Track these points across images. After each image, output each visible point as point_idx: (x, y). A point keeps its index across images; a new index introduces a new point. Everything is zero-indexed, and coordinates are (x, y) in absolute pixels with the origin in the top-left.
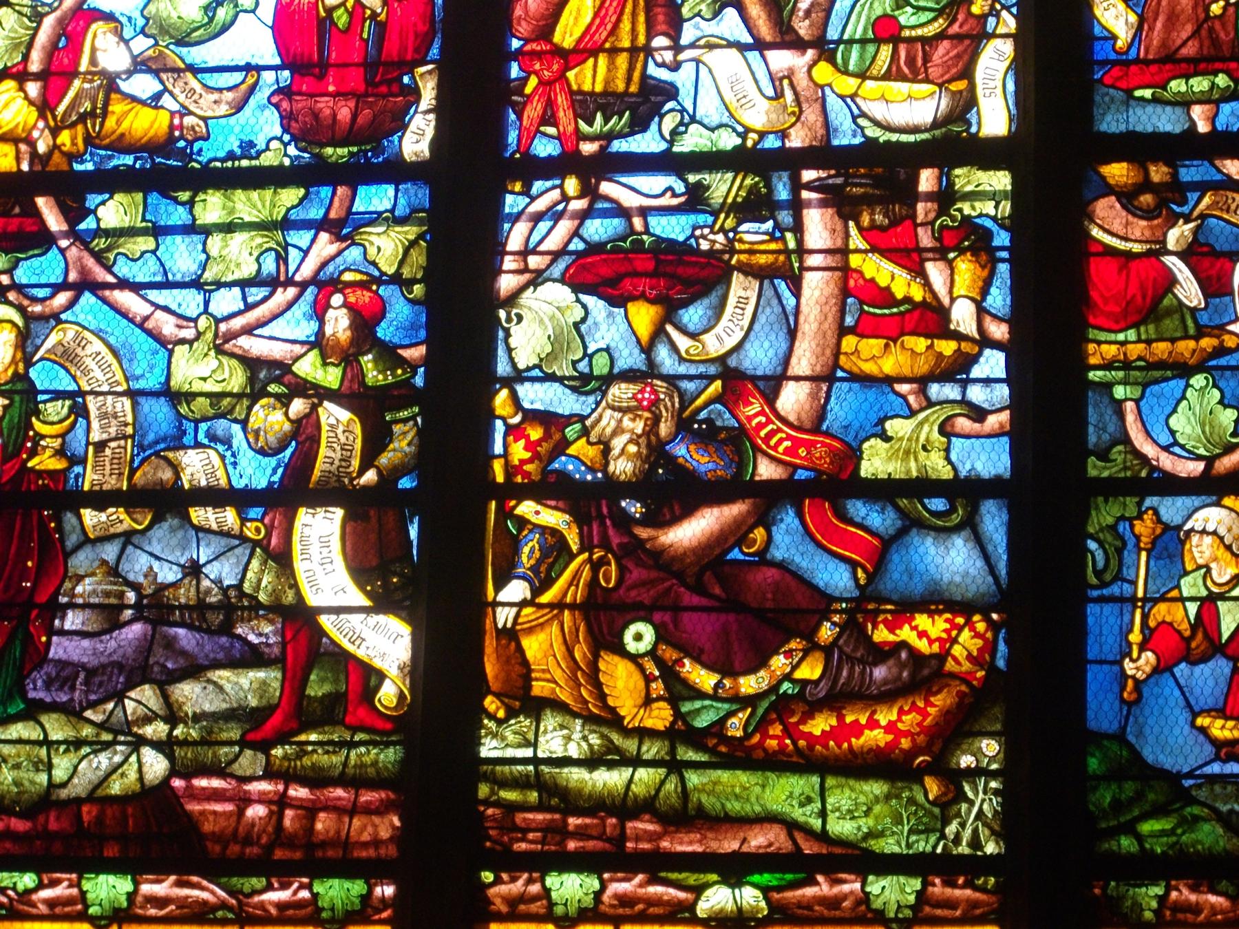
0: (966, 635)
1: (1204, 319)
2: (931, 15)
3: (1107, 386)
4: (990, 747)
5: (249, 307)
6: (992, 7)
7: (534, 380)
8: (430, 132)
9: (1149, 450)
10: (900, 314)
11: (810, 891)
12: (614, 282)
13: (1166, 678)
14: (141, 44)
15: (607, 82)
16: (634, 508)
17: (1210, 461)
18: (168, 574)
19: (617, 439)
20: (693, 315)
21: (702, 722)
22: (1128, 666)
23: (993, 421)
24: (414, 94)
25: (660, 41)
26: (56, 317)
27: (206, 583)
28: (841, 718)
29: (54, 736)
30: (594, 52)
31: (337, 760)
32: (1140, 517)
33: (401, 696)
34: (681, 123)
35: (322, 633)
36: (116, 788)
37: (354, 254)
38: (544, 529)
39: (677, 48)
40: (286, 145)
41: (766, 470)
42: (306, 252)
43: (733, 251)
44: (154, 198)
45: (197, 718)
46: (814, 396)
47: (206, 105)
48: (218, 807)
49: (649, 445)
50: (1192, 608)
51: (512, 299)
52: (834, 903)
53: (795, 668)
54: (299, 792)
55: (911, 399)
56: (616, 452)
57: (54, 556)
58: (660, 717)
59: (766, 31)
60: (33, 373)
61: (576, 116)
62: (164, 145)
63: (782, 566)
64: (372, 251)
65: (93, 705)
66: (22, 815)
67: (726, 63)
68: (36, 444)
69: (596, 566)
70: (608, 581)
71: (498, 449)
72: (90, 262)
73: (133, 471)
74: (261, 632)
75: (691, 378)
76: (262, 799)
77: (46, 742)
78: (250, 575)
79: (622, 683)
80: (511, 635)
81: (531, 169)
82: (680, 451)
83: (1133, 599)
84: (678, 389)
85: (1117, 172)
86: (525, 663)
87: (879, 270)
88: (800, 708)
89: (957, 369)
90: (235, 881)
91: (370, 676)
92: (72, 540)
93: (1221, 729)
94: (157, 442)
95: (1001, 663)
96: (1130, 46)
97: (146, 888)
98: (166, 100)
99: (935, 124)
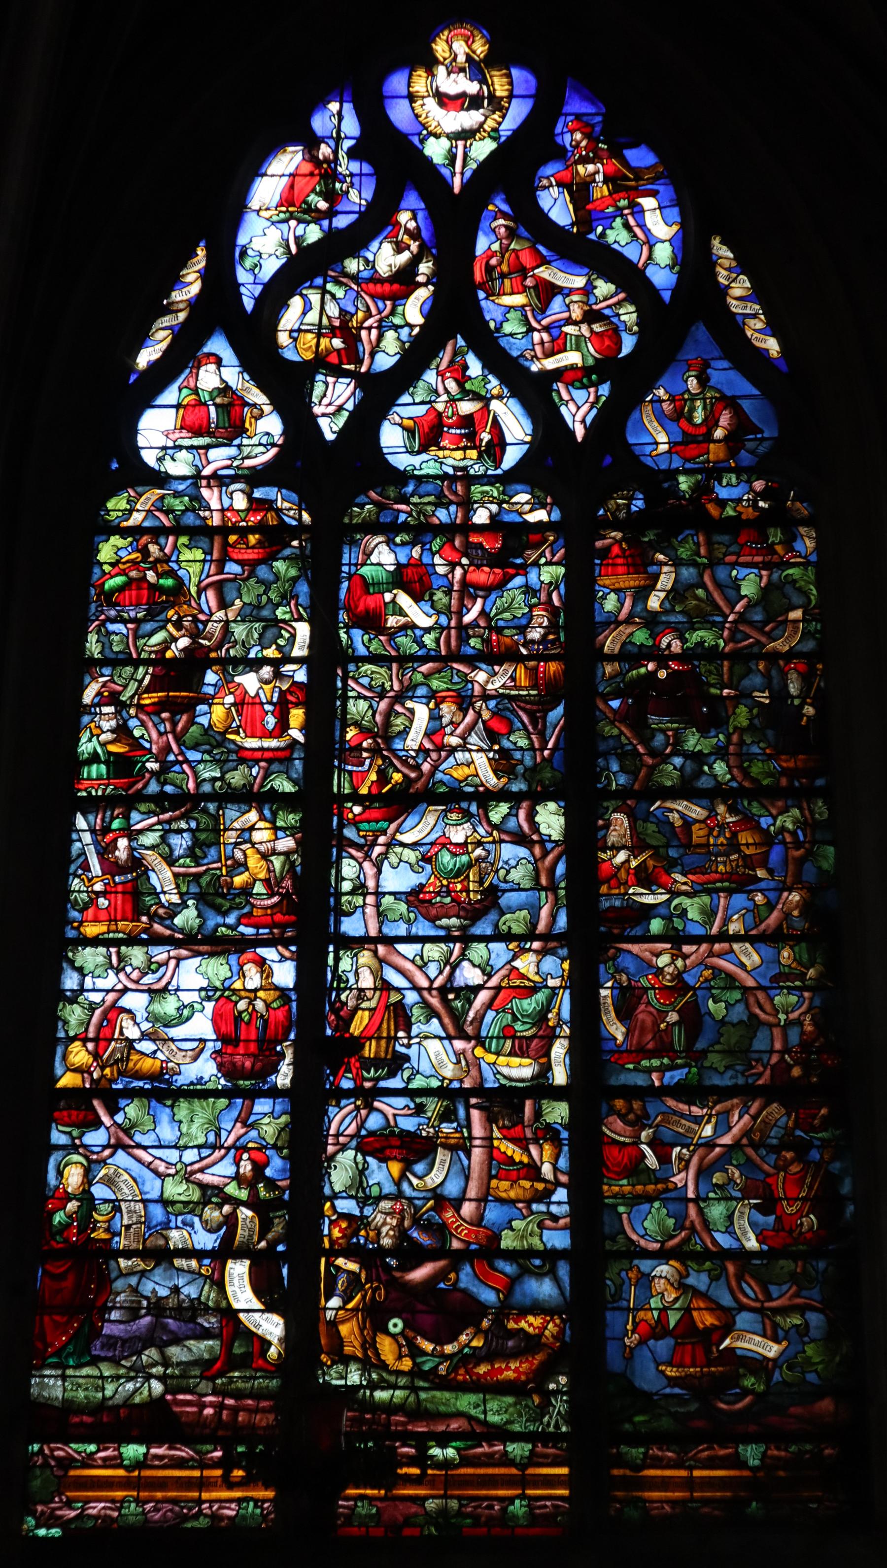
0: (550, 1326)
1: (658, 1175)
3: (615, 1206)
4: (563, 1380)
5: (202, 1159)
9: (634, 1237)
11: (480, 1450)
13: (645, 1347)
14: (146, 1026)
15: (376, 1052)
16: (393, 1263)
17: (663, 1243)
18: (163, 1292)
20: (419, 1168)
21: (426, 1367)
23: (562, 1222)
24: (282, 1056)
25: (401, 1034)
26: (104, 1162)
29: (106, 1374)
30: (370, 1039)
31: (249, 1385)
33: (279, 1354)
35: (241, 1322)
36: (137, 1399)
37: (253, 1134)
38: (349, 1272)
39: (410, 1038)
41: (456, 1245)
44: (154, 1103)
45: (179, 1364)
46: (478, 1208)
47: (179, 1058)
48: (188, 1409)
50: (656, 1313)
52: (490, 1455)
54: (230, 1402)
57: (105, 1283)
58: (407, 1364)
60: (93, 1189)
63: (465, 1291)
64: (262, 1133)
65: (126, 1358)
66: (90, 1414)
67: (434, 1046)
69: (375, 1290)
71: (326, 1232)
73: (145, 1240)
74: (209, 1322)
76: (211, 1405)
77: (102, 1377)
80: (333, 1325)
81: (340, 1094)
82: (415, 1235)
83: (628, 1309)
85: (619, 1103)
86: (340, 1338)
87: (509, 1148)
89: (544, 1196)
90: (199, 1447)
91: (266, 1344)
92: (114, 1275)
93: (671, 1372)
95: (567, 1339)
97: (153, 1451)
98: (159, 1055)
99: (533, 1078)
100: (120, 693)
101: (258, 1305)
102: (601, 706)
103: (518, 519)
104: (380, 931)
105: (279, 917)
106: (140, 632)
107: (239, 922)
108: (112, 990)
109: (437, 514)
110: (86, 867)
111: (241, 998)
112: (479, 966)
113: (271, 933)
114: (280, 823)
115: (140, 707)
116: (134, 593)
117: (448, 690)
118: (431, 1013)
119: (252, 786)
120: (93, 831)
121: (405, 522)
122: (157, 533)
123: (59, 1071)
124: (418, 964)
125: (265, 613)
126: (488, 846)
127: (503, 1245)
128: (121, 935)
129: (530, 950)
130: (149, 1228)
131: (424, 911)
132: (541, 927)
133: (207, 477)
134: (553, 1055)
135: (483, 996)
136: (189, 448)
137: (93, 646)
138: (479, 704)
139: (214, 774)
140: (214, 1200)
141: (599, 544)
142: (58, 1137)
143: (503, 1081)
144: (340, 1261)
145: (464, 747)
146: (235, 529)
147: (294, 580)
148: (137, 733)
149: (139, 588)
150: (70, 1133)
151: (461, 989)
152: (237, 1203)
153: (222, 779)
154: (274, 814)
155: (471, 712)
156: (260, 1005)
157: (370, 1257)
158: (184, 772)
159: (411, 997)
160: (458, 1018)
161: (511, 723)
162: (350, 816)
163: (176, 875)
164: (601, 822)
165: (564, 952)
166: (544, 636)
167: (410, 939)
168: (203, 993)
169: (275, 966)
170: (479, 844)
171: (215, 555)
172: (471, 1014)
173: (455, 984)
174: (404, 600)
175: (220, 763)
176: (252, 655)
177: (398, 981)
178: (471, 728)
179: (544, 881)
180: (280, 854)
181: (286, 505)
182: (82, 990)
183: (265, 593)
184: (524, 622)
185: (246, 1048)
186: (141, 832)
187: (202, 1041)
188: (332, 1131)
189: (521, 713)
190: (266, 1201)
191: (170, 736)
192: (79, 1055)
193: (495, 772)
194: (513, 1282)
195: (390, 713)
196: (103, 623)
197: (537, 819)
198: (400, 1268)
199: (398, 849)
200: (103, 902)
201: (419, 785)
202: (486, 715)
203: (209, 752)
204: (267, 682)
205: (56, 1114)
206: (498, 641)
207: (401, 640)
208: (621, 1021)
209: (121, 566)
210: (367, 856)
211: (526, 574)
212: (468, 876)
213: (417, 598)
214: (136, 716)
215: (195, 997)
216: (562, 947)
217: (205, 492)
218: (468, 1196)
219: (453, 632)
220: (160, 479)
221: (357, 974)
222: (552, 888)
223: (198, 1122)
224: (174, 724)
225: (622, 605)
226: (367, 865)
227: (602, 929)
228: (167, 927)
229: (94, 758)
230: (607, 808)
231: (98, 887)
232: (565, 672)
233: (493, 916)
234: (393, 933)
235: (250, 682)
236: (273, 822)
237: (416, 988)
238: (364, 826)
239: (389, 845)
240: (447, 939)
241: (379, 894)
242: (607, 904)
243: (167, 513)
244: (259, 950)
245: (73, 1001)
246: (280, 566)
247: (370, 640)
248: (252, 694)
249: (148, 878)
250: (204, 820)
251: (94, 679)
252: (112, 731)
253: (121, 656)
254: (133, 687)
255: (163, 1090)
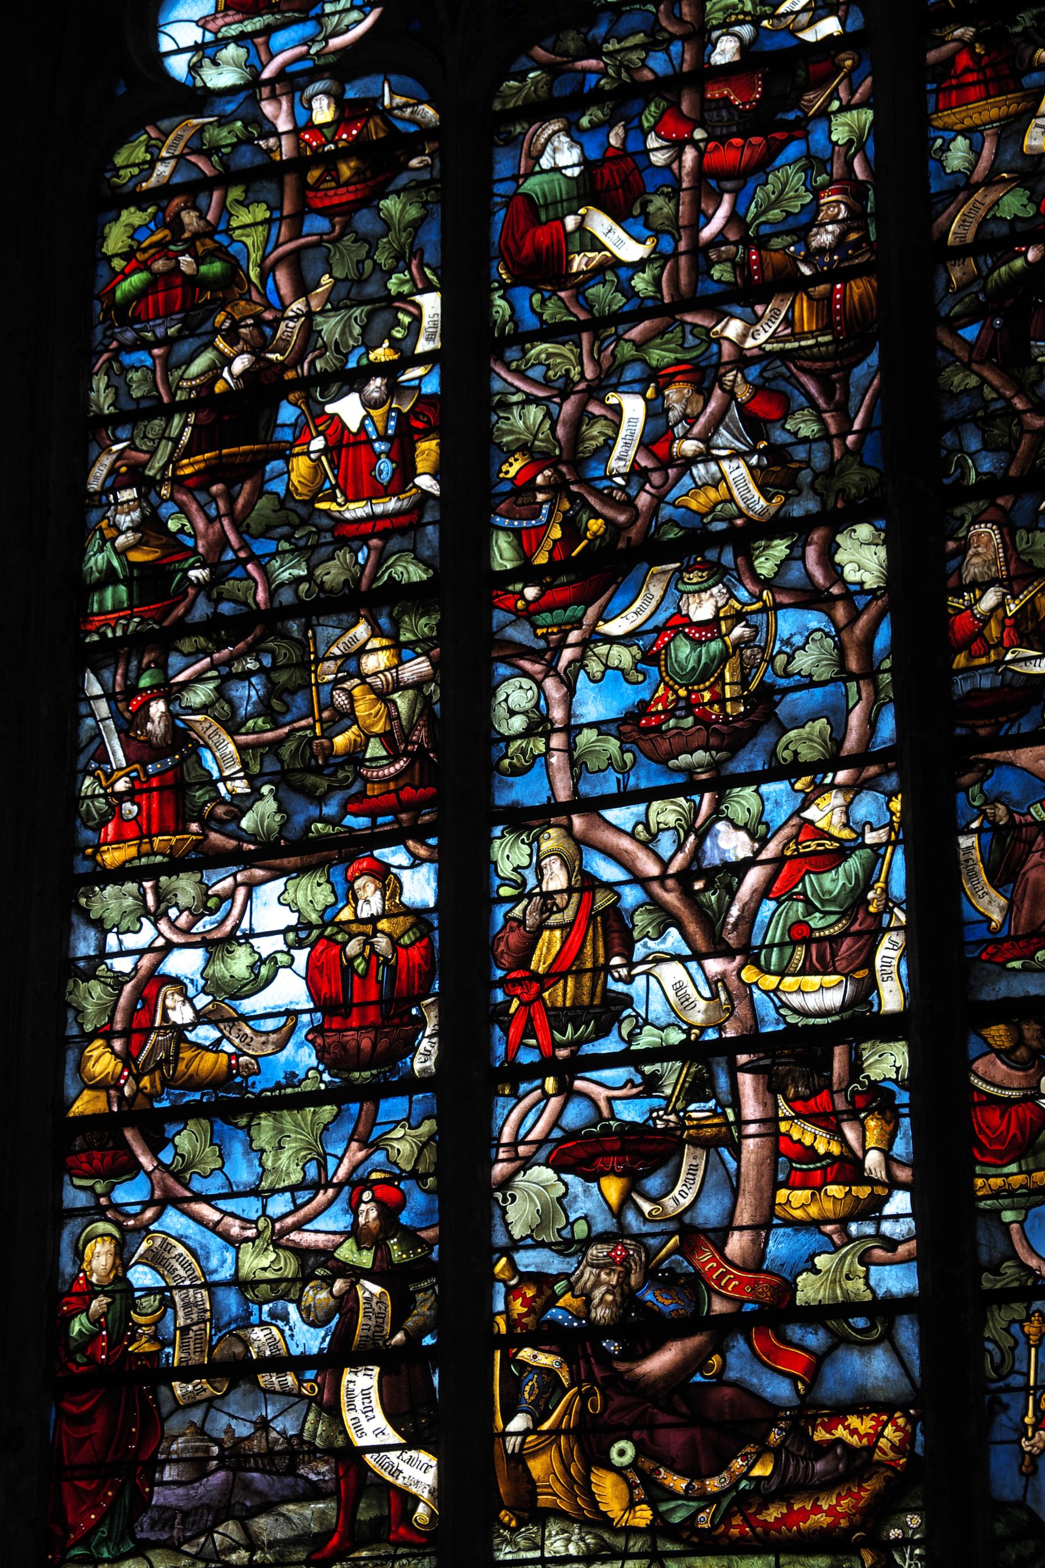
0: (889, 1431)
2: (833, 918)
3: (997, 1212)
4: (914, 1521)
5: (298, 1208)
6: (886, 905)
7: (527, 1247)
8: (434, 1052)
10: (823, 1168)
12: (589, 1161)
14: (202, 1001)
15: (575, 997)
18: (243, 1430)
19: (596, 1290)
20: (654, 1183)
21: (677, 1518)
22: (1024, 1443)
23: (902, 1249)
24: (421, 1022)
25: (616, 961)
26: (144, 1230)
27: (273, 1435)
28: (790, 1507)
30: (563, 976)
32: (1028, 1319)
33: (432, 1515)
34: (636, 1026)
37: (379, 1157)
40: (321, 1073)
41: (719, 1306)
42: (341, 1160)
43: (685, 1128)
44: (219, 1124)
45: (271, 1544)
49: (622, 1294)
51: (507, 1182)
53: (751, 1468)
55: (835, 1237)
56: (596, 1301)
57: (152, 1424)
58: (643, 1516)
59: (701, 944)
61: (552, 1028)
62: (226, 1079)
63: (734, 1384)
64: (393, 1154)
65: (188, 1540)
67: (671, 973)
68: (135, 1332)
69: (584, 1397)
70: (594, 1408)
72: (170, 1181)
73: (212, 1349)
74: (319, 1472)
75: (654, 1235)
78: (307, 1425)
79: (609, 1492)
80: (519, 1459)
81: (516, 1075)
82: (649, 1296)
83: (1026, 1388)
84: (644, 1245)
88: (758, 1500)
89: (872, 1209)
92: (165, 1410)
94: (229, 1324)
95: (919, 1450)
96: (1002, 925)
99: (844, 1007)
100: (145, 465)
101: (393, 1437)
102: (947, 341)
103: (789, 43)
104: (575, 791)
105: (407, 794)
106: (174, 359)
107: (345, 811)
108: (150, 949)
109: (651, 63)
110: (102, 757)
111: (352, 936)
112: (744, 828)
113: (397, 821)
114: (405, 636)
115: (178, 482)
116: (161, 296)
117: (678, 362)
118: (667, 919)
119: (358, 581)
120: (109, 696)
121: (597, 89)
122: (194, 190)
123: (71, 1091)
124: (640, 836)
125: (371, 289)
126: (756, 619)
127: (800, 1298)
128: (159, 859)
129: (833, 786)
130: (219, 1329)
131: (647, 746)
132: (851, 743)
133: (270, 82)
134: (878, 963)
135: (754, 877)
136: (240, 39)
137: (102, 396)
138: (730, 377)
139: (296, 572)
140: (319, 1272)
141: (932, 56)
142: (75, 1197)
143: (793, 1019)
144: (526, 1354)
145: (706, 456)
146: (319, 158)
147: (416, 225)
148: (173, 525)
149: (169, 287)
150: (91, 1189)
151: (716, 870)
152: (354, 1273)
153: (309, 578)
154: (396, 623)
155: (718, 392)
156: (382, 943)
157: (574, 1342)
158: (250, 577)
159: (631, 896)
160: (711, 921)
161: (786, 399)
162: (520, 604)
163: (241, 748)
164: (951, 545)
165: (892, 782)
166: (840, 239)
167: (623, 798)
168: (291, 936)
169: (405, 876)
170: (738, 617)
171: (287, 209)
172: (735, 911)
173: (705, 864)
174: (600, 224)
175: (304, 551)
176: (352, 364)
177: (608, 871)
178: (718, 421)
179: (853, 665)
180: (407, 687)
181: (399, 100)
182: (103, 955)
183: (369, 255)
184: (804, 219)
185: (363, 1017)
186: (185, 685)
187: (291, 1014)
188: (506, 1138)
189: (804, 379)
190: (400, 1265)
191: (226, 522)
192: (102, 1062)
193: (761, 489)
194: (820, 1360)
195: (581, 417)
196: (116, 352)
197: (839, 558)
198: (624, 1357)
199: (602, 649)
200: (130, 809)
201: (633, 533)
202: (743, 393)
203: (288, 538)
204: (376, 405)
205: (70, 1160)
206: (760, 261)
207: (596, 291)
208: (996, 888)
209: (140, 256)
210: (551, 669)
211: (806, 136)
212: (722, 675)
213: (619, 217)
214: (172, 498)
215: (277, 943)
216: (887, 772)
217: (268, 108)
218: (737, 1222)
219: (683, 261)
220: (196, 99)
221: (539, 871)
222: (870, 673)
223: (290, 1147)
224: (231, 500)
225: (978, 155)
226: (550, 684)
227: (959, 731)
228: (229, 836)
229: (109, 577)
230: (962, 518)
231: (121, 786)
232: (879, 293)
233: (765, 738)
234: (598, 791)
235: (349, 410)
236: (394, 636)
237: (638, 879)
238: (546, 618)
239: (585, 644)
240: (690, 787)
241: (571, 730)
242: (967, 687)
243: (207, 154)
244: (377, 853)
245: (89, 975)
246: (391, 205)
247: (543, 302)
248: (354, 427)
249: (199, 760)
250: (285, 652)
251: (105, 449)
252: (134, 529)
253: (145, 404)
254: (165, 449)
255: (233, 1102)
